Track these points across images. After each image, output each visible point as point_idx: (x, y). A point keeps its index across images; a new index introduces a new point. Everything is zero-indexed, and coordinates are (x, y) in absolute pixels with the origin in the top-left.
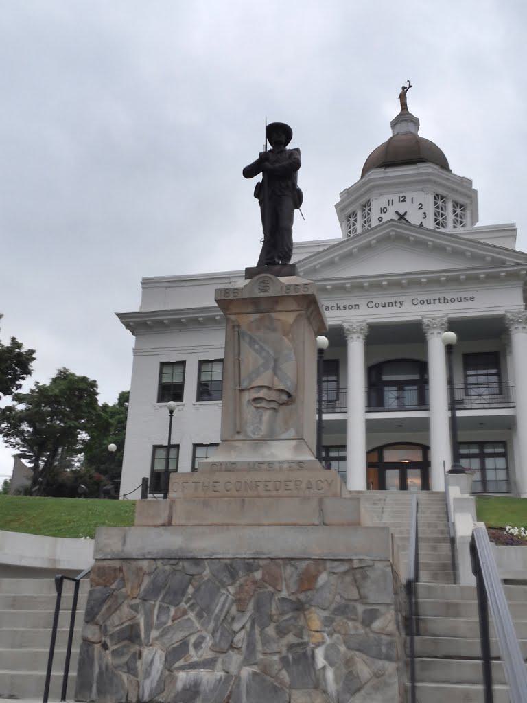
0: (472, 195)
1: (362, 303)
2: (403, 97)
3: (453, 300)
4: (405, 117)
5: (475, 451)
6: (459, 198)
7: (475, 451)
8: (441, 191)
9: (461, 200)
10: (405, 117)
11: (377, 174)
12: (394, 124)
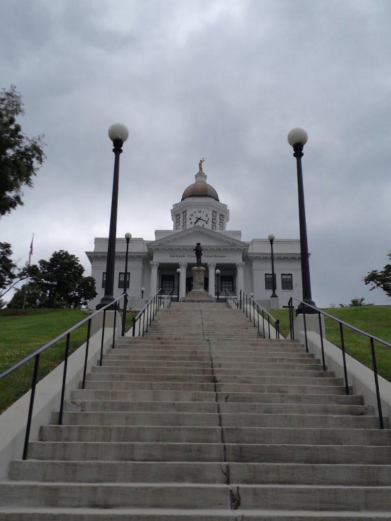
1: (186, 255)
2: (200, 165)
4: (201, 174)
6: (222, 214)
8: (215, 210)
10: (201, 174)
11: (189, 200)
12: (196, 176)
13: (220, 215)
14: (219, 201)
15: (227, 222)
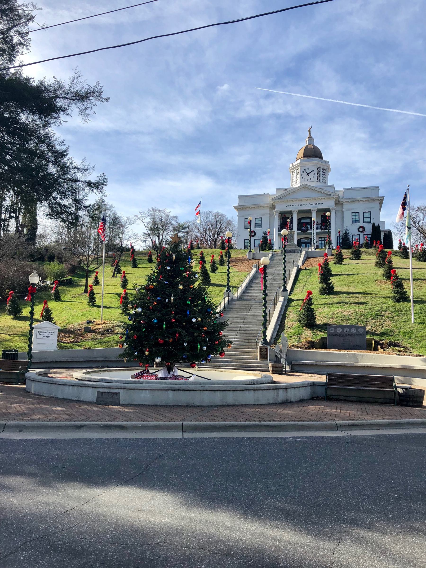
0: (329, 167)
2: (310, 131)
3: (318, 204)
4: (310, 138)
5: (323, 239)
7: (323, 239)
9: (325, 168)
13: (323, 169)
14: (321, 158)
15: (328, 172)
